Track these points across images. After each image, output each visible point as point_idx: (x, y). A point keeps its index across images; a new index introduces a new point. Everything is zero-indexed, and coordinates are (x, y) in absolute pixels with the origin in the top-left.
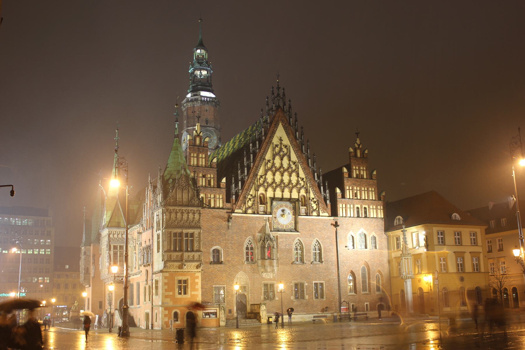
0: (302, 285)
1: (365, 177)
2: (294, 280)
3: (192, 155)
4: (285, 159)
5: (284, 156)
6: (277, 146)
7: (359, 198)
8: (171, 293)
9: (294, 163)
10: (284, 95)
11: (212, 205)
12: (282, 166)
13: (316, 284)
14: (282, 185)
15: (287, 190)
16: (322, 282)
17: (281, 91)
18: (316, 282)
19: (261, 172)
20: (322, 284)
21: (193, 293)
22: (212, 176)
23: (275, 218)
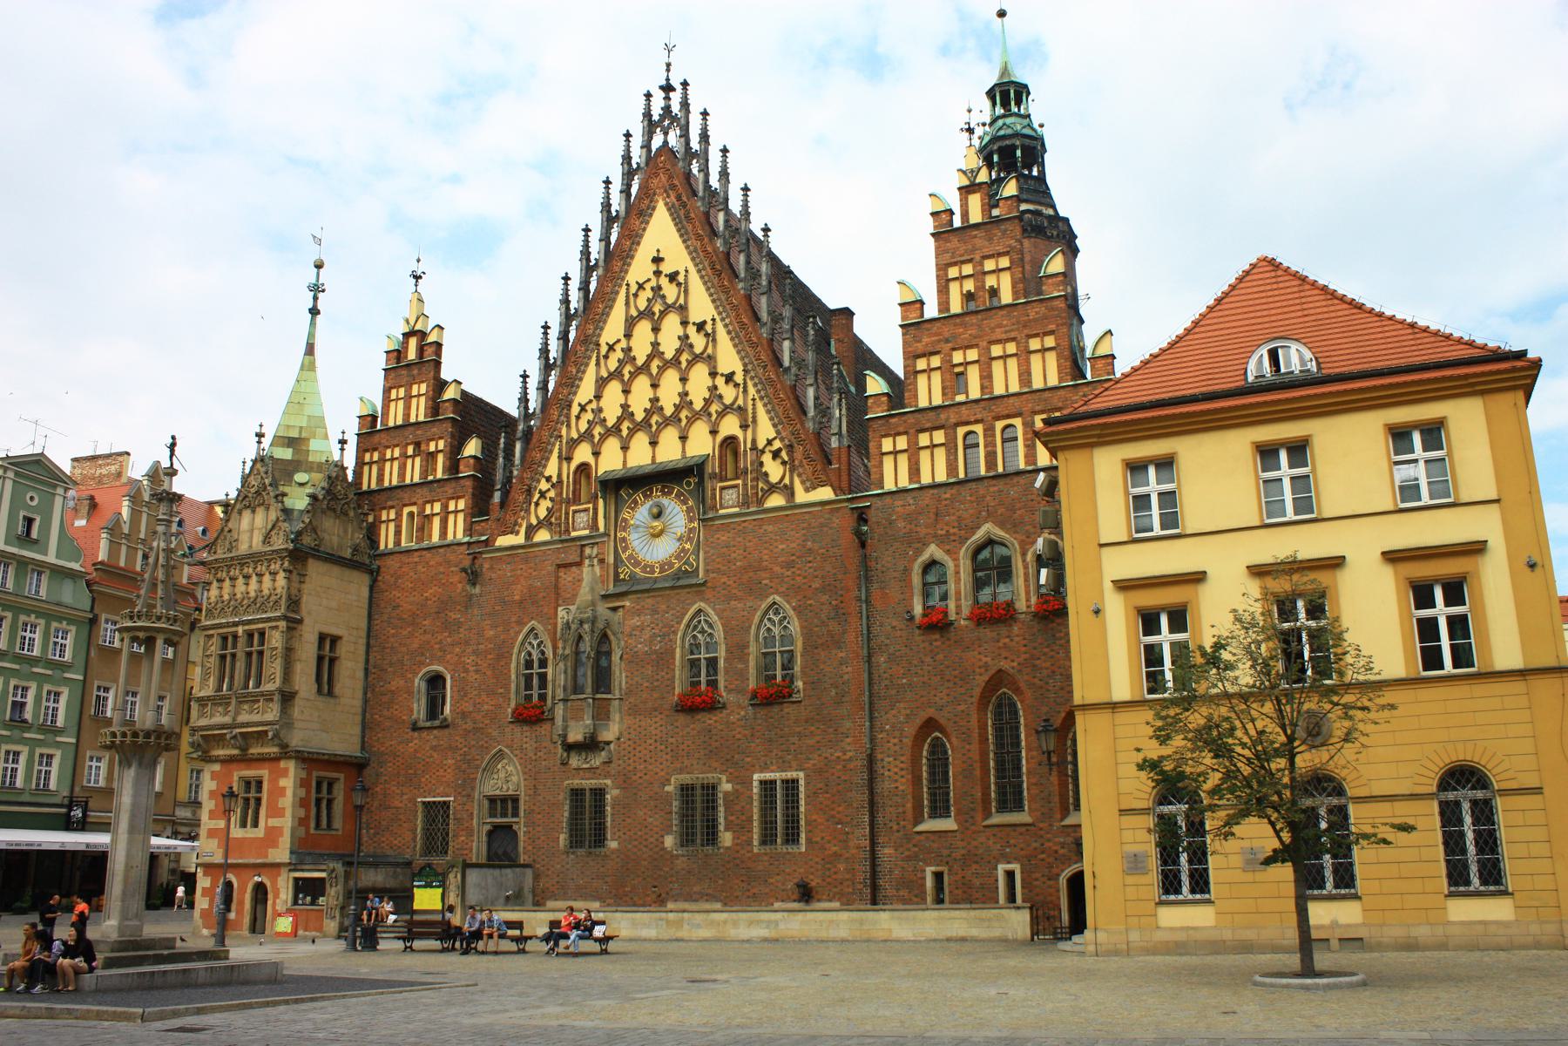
0: (710, 790)
1: (1006, 297)
2: (681, 771)
3: (394, 392)
4: (672, 324)
5: (663, 314)
6: (641, 286)
7: (975, 392)
8: (222, 824)
9: (700, 327)
10: (685, 105)
11: (435, 538)
12: (656, 352)
13: (768, 786)
14: (652, 423)
15: (669, 437)
16: (790, 775)
17: (676, 98)
18: (768, 776)
19: (586, 391)
20: (791, 785)
21: (273, 822)
22: (441, 445)
23: (624, 540)
